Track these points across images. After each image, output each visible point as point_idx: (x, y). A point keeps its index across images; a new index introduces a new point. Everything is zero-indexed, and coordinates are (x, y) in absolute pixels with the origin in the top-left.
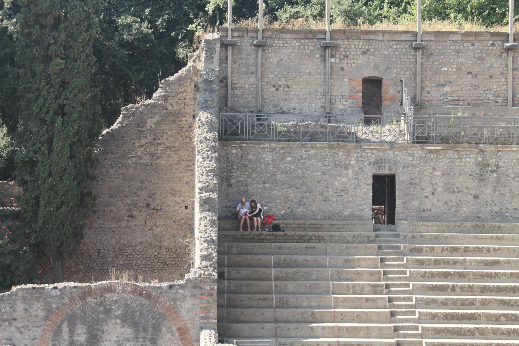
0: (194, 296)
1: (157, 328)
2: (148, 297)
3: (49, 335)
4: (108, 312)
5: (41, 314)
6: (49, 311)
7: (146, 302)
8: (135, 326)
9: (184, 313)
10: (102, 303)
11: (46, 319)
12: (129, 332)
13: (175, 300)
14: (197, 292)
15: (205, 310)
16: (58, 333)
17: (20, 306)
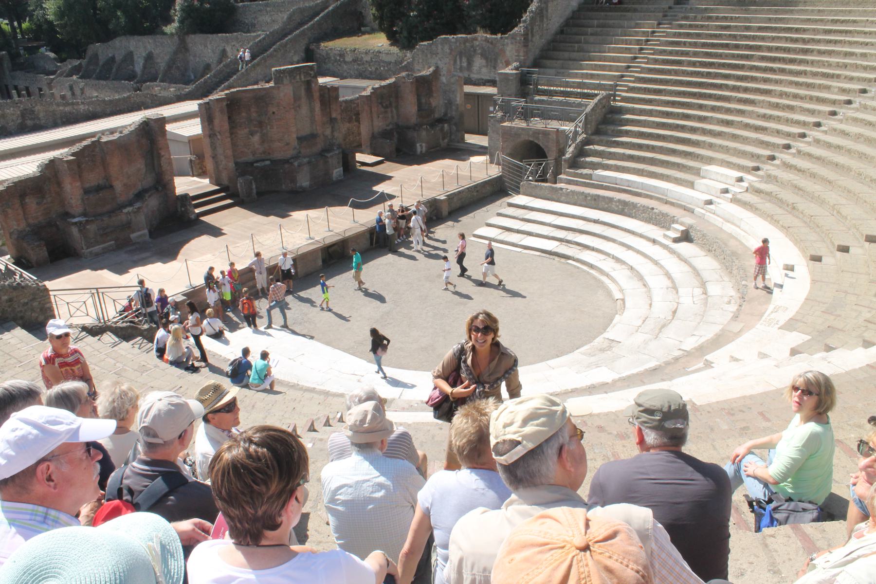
0: (512, 43)
1: (496, 60)
2: (492, 43)
3: (452, 62)
4: (475, 51)
5: (448, 51)
6: (451, 50)
7: (491, 46)
8: (486, 59)
9: (508, 53)
10: (472, 46)
11: (450, 53)
12: (483, 62)
13: (503, 45)
14: (514, 41)
15: (518, 51)
16: (455, 61)
17: (440, 47)
